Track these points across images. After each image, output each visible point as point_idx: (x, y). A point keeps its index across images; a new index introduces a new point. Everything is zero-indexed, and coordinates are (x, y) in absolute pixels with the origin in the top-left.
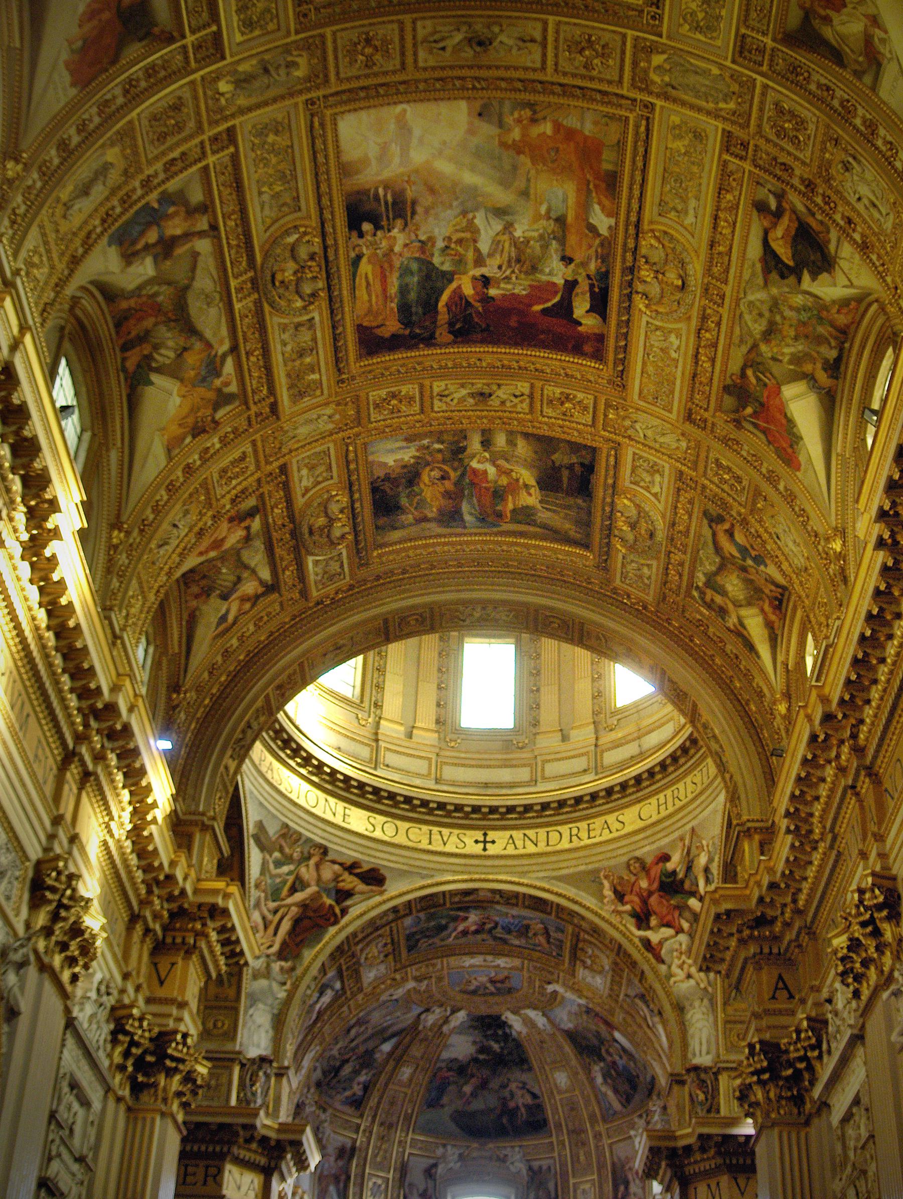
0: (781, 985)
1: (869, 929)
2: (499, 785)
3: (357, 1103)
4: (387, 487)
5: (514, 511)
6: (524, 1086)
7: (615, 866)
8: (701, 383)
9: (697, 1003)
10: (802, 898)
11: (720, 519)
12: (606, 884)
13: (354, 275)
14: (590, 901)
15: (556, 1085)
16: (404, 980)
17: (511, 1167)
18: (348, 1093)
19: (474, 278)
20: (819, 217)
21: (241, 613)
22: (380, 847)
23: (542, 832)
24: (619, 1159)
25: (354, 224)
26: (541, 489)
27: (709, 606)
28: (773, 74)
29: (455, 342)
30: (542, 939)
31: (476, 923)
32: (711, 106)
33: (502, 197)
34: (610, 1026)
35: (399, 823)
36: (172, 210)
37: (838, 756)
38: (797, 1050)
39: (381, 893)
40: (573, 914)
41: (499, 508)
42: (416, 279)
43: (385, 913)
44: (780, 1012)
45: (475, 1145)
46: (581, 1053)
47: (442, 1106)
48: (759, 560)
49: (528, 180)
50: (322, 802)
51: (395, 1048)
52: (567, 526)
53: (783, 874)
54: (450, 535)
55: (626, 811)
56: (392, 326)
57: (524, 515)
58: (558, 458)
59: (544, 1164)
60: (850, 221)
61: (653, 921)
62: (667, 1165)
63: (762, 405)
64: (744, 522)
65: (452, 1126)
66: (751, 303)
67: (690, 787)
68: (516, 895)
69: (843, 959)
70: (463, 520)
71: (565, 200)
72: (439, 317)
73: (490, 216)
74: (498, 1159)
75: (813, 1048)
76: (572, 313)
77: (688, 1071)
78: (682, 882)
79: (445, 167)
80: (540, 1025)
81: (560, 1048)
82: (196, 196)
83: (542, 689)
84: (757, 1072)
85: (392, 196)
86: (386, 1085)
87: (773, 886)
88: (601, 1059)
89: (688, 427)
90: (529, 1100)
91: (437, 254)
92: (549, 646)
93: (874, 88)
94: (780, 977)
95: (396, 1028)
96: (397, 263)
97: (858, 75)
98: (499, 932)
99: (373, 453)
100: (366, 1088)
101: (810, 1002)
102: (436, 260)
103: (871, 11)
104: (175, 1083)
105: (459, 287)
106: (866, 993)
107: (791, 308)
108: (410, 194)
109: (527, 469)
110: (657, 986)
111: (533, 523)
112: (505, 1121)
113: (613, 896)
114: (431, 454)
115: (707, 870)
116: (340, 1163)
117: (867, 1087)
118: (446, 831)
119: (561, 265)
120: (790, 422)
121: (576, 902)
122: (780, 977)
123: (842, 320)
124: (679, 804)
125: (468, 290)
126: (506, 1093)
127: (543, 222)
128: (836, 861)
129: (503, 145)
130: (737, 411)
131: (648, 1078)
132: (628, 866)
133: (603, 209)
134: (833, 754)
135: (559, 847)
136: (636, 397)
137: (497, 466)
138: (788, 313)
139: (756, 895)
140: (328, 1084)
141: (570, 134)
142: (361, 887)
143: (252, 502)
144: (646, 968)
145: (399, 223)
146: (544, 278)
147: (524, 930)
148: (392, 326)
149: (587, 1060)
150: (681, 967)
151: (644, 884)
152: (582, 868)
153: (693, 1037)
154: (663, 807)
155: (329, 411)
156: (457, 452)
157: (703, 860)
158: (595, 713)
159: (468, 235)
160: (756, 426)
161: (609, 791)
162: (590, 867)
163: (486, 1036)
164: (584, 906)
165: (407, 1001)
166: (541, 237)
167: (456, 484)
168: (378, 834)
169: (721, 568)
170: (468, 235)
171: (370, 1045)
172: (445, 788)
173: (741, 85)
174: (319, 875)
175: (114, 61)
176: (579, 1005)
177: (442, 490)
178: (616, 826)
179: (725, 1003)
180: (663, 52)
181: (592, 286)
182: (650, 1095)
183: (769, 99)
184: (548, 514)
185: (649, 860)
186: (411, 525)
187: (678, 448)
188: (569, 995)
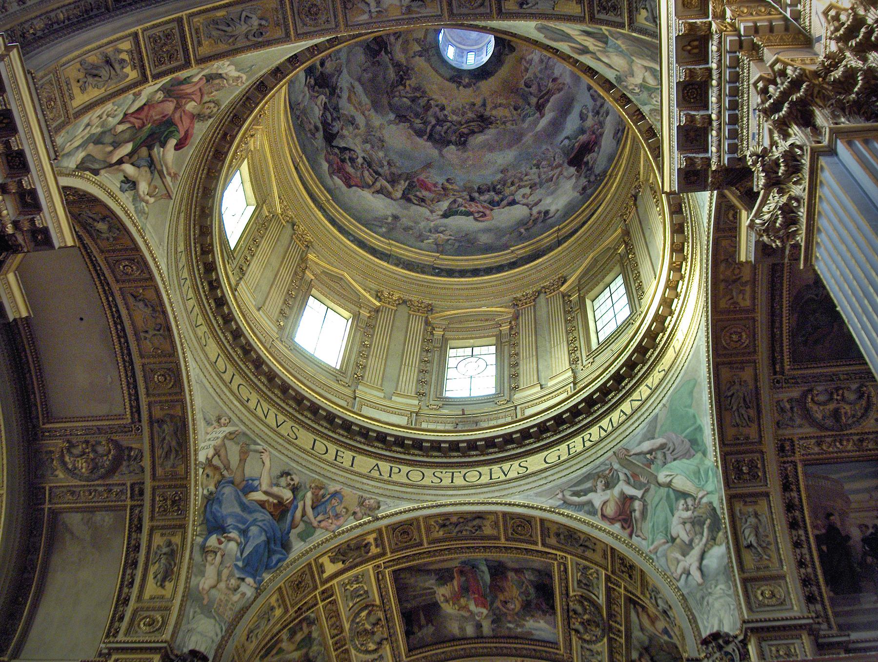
4: (544, 606)
5: (452, 578)
26: (437, 602)
41: (463, 579)
52: (412, 581)
57: (444, 576)
58: (431, 629)
61: (160, 96)
70: (489, 568)
99: (555, 634)
109: (450, 614)
111: (438, 572)
113: (220, 72)
114: (516, 621)
137: (469, 611)
157: (143, 187)
167: (496, 597)
177: (506, 593)
184: (427, 585)
186: (527, 569)
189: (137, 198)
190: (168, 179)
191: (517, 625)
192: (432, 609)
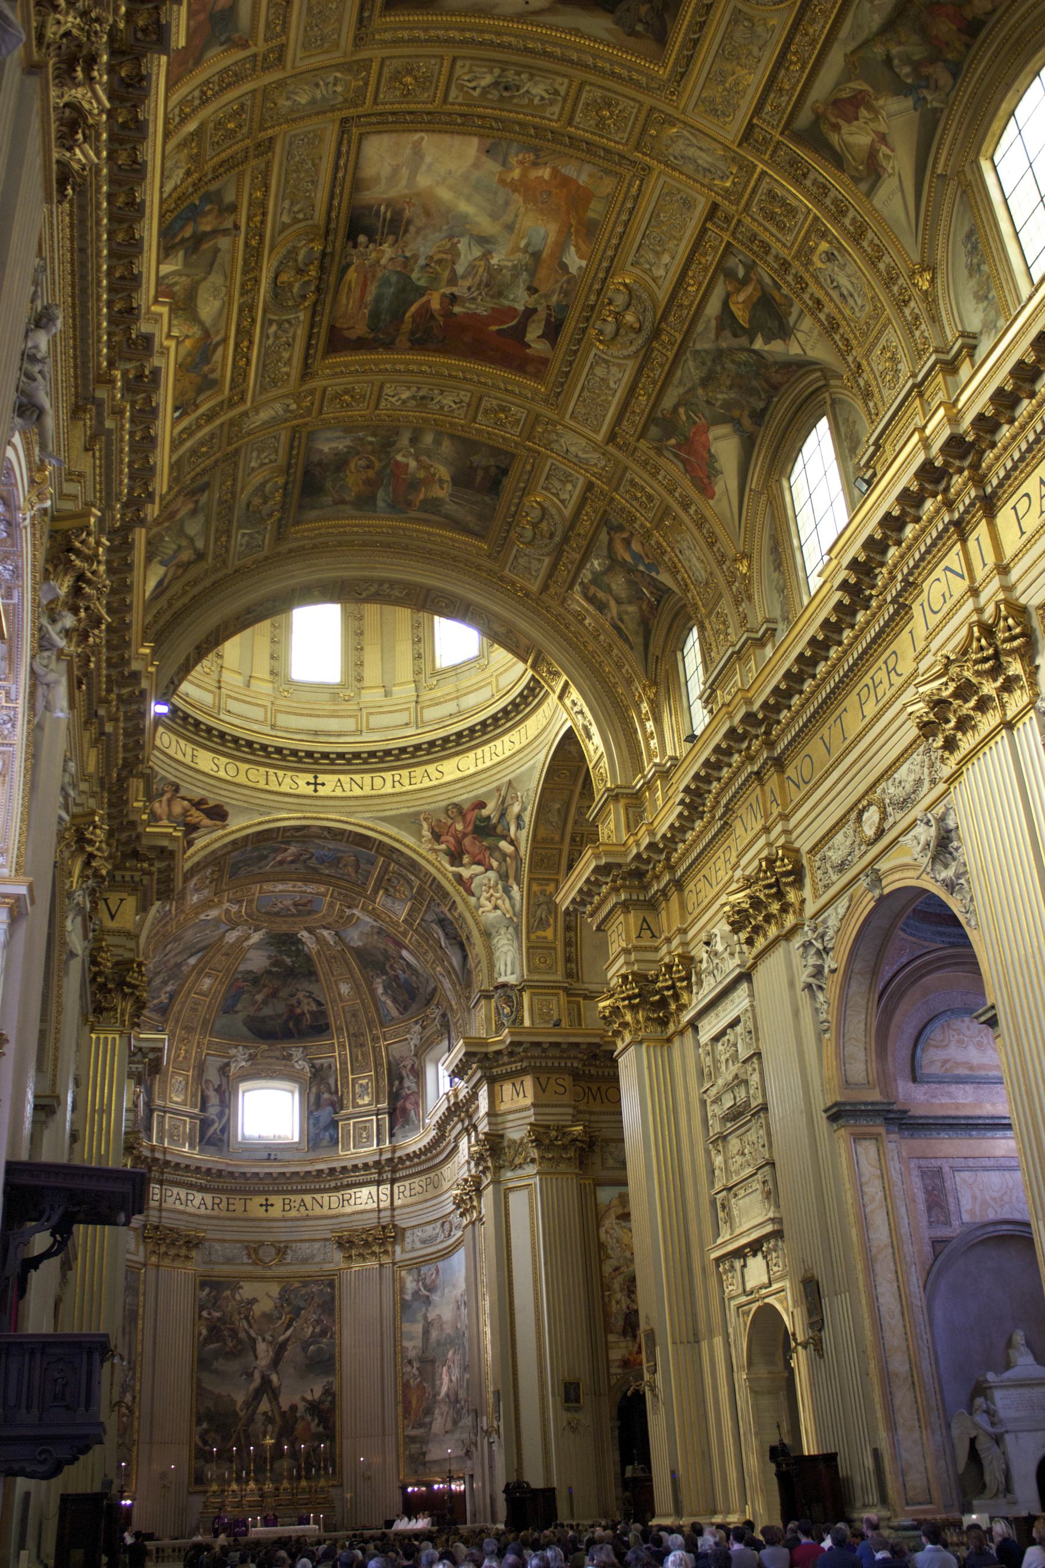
0: (645, 926)
1: (774, 890)
2: (329, 734)
5: (424, 502)
6: (310, 995)
7: (435, 810)
8: (634, 412)
9: (503, 931)
10: (675, 856)
11: (620, 528)
12: (425, 825)
13: (341, 279)
14: (410, 841)
15: (339, 994)
16: (220, 902)
19: (444, 295)
20: (785, 290)
21: (175, 578)
22: (224, 786)
23: (367, 777)
25: (352, 236)
27: (591, 600)
28: (773, 163)
29: (411, 349)
30: (351, 870)
31: (293, 854)
32: (706, 181)
33: (486, 226)
34: (400, 945)
35: (239, 764)
36: (208, 207)
37: (749, 748)
38: (666, 980)
39: (224, 827)
40: (393, 850)
42: (392, 290)
43: (225, 845)
44: (646, 949)
45: (266, 1047)
48: (649, 567)
49: (517, 216)
50: (174, 743)
53: (664, 836)
54: (360, 518)
55: (445, 762)
56: (361, 329)
58: (476, 459)
59: (325, 1062)
60: (818, 302)
61: (466, 859)
62: (478, 1068)
63: (687, 439)
64: (648, 534)
65: (245, 1031)
66: (697, 352)
67: (508, 744)
68: (343, 832)
69: (739, 912)
70: (375, 505)
71: (545, 238)
72: (404, 326)
73: (473, 242)
74: (284, 1058)
75: (682, 979)
76: (524, 336)
77: (497, 988)
78: (495, 827)
79: (445, 194)
81: (347, 964)
82: (229, 197)
83: (366, 648)
84: (629, 998)
85: (393, 213)
86: (189, 992)
87: (652, 846)
88: (384, 972)
89: (610, 448)
90: (314, 1007)
91: (416, 269)
92: (371, 611)
93: (870, 193)
94: (644, 920)
96: (379, 275)
97: (856, 180)
98: (313, 863)
100: (172, 997)
101: (675, 942)
102: (414, 276)
103: (883, 128)
104: (129, 1006)
105: (428, 302)
106: (760, 943)
107: (733, 362)
108: (407, 214)
110: (467, 915)
112: (291, 1025)
115: (519, 817)
117: (750, 1014)
118: (280, 773)
119: (526, 295)
120: (712, 456)
121: (397, 840)
122: (644, 920)
123: (777, 378)
124: (496, 760)
125: (435, 305)
126: (294, 1001)
127: (520, 255)
128: (719, 831)
129: (502, 181)
130: (660, 440)
131: (429, 989)
132: (446, 810)
133: (577, 252)
134: (745, 745)
135: (382, 791)
136: (568, 416)
138: (729, 365)
139: (634, 851)
141: (565, 182)
142: (206, 821)
143: (205, 479)
144: (458, 899)
145: (391, 239)
146: (507, 303)
147: (335, 861)
148: (361, 329)
150: (489, 899)
151: (460, 827)
152: (405, 810)
153: (498, 959)
154: (480, 761)
155: (287, 401)
156: (387, 445)
157: (516, 808)
158: (417, 672)
159: (449, 257)
160: (676, 455)
161: (432, 744)
162: (412, 810)
163: (280, 952)
164: (404, 844)
165: (217, 921)
166: (515, 267)
168: (222, 774)
169: (609, 570)
170: (449, 257)
171: (179, 959)
172: (279, 734)
173: (741, 168)
174: (170, 810)
175: (198, 62)
176: (373, 927)
177: (364, 477)
178: (435, 775)
179: (528, 933)
180: (674, 126)
181: (549, 316)
182: (428, 1002)
183: (764, 184)
184: (455, 507)
185: (466, 807)
187: (596, 465)
188: (368, 919)
189: (524, 809)
190: (503, 793)
191: (362, 439)
192: (463, 479)
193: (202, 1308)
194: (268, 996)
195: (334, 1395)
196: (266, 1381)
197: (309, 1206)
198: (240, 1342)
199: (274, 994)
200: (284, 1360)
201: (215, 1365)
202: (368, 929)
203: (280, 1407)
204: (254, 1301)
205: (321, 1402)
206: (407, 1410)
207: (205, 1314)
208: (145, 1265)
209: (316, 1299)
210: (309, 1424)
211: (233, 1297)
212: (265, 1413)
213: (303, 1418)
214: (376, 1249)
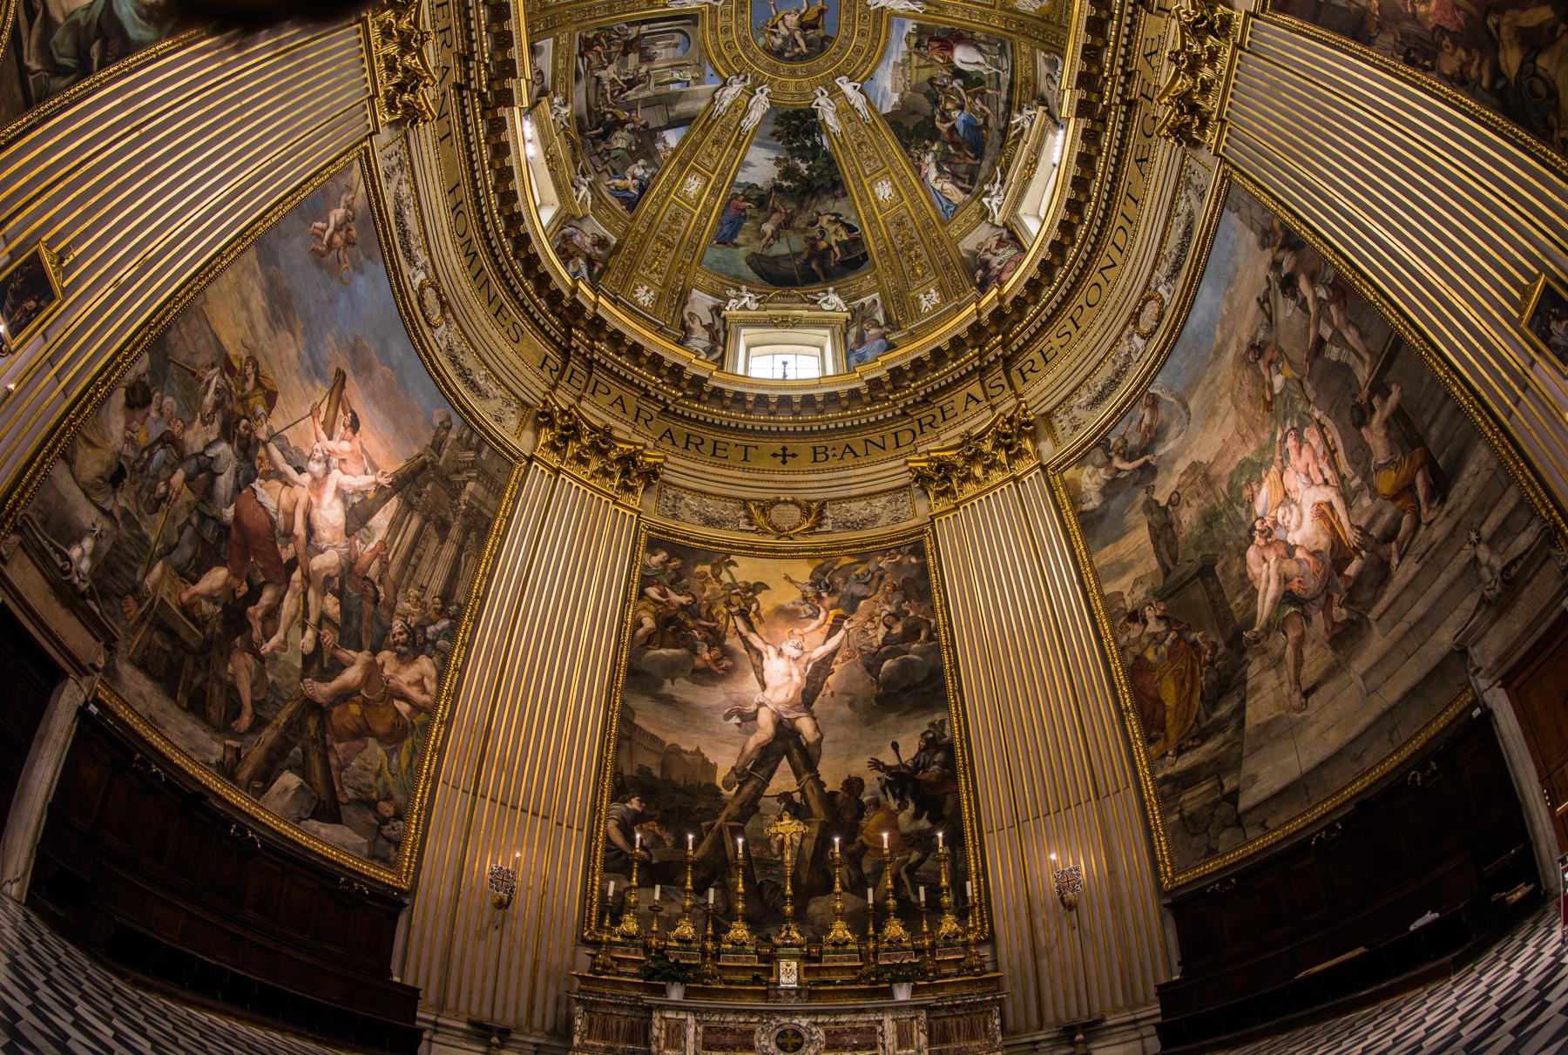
3: (631, 204)
6: (837, 218)
15: (877, 202)
17: (826, 307)
18: (617, 182)
24: (968, 251)
46: (907, 147)
47: (737, 246)
51: (681, 145)
59: (867, 300)
65: (748, 272)
80: (858, 105)
88: (934, 135)
95: (682, 108)
112: (814, 266)
116: (599, 252)
126: (815, 232)
140: (595, 145)
149: (916, 153)
163: (791, 151)
171: (653, 118)
193: (646, 581)
194: (779, 226)
195: (949, 749)
196: (785, 732)
197: (859, 449)
198: (728, 653)
199: (786, 224)
200: (826, 691)
201: (668, 688)
202: (899, 50)
203: (822, 785)
204: (760, 587)
205: (918, 765)
206: (1152, 722)
207: (653, 592)
208: (530, 459)
209: (888, 578)
210: (892, 816)
211: (717, 576)
212: (785, 797)
213: (877, 804)
214: (1002, 456)
